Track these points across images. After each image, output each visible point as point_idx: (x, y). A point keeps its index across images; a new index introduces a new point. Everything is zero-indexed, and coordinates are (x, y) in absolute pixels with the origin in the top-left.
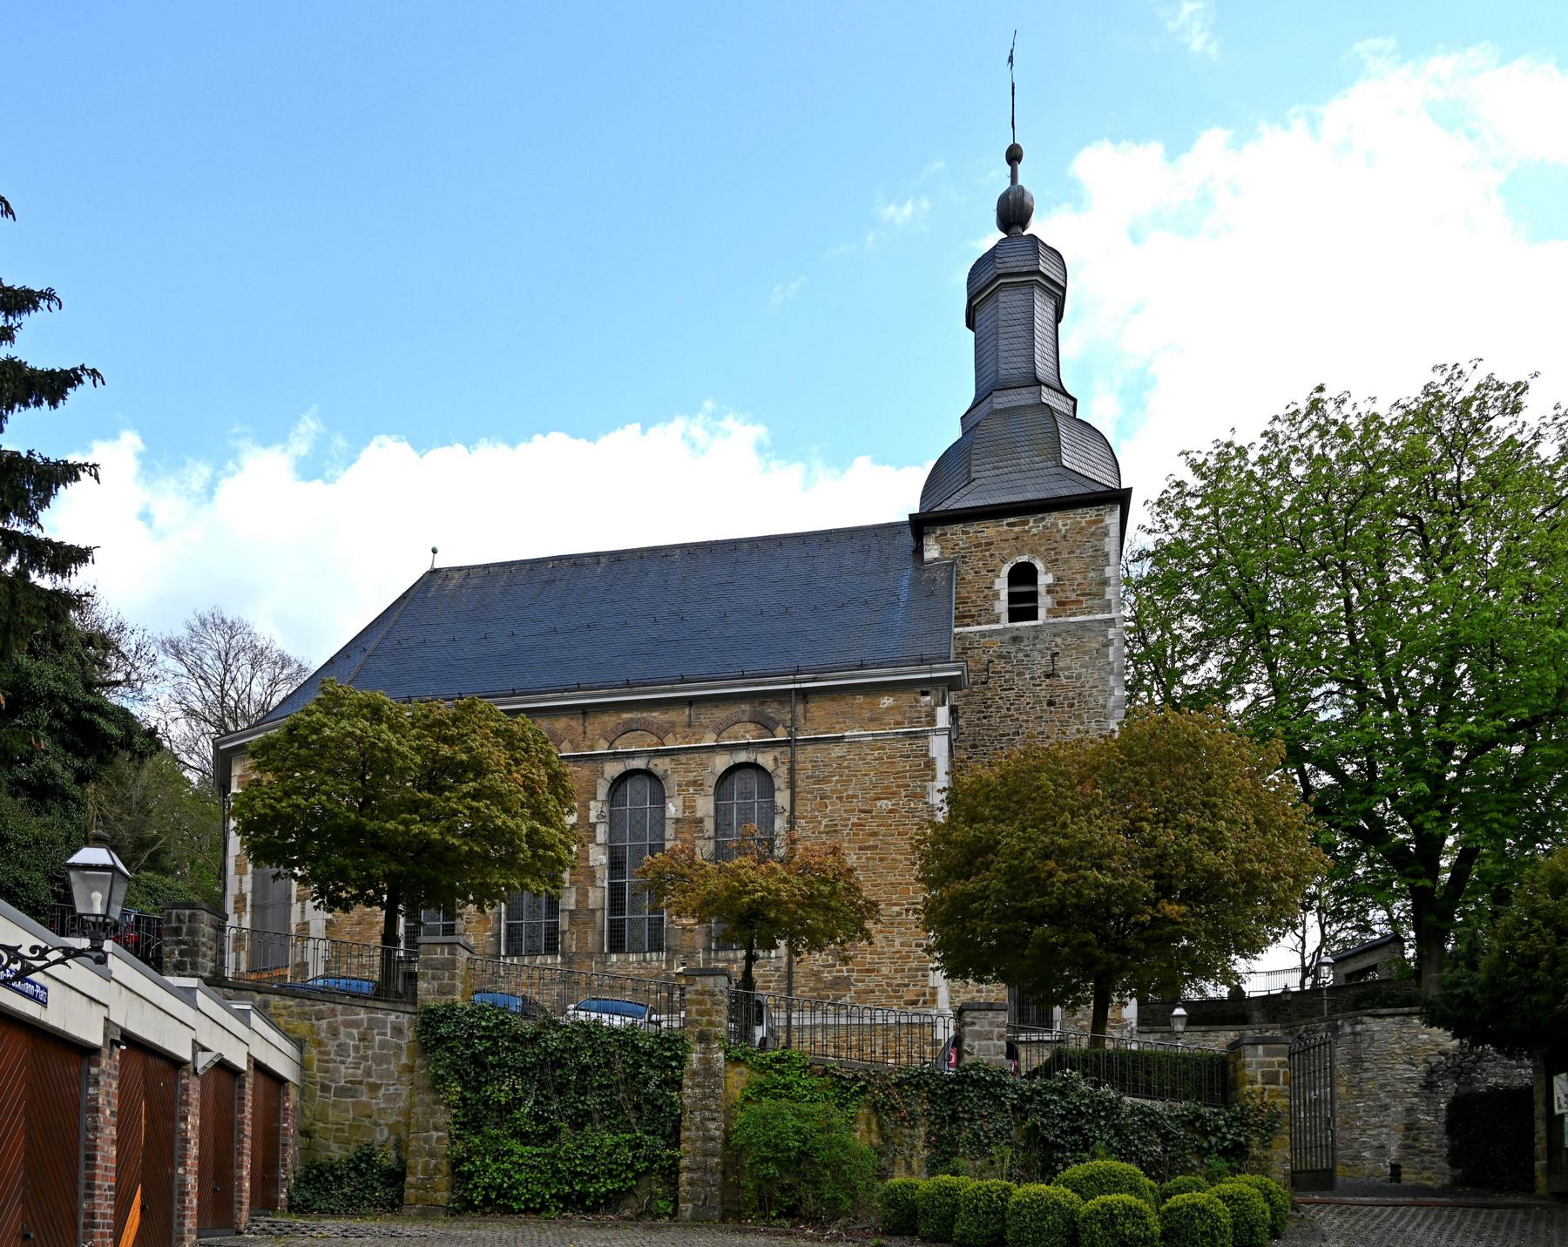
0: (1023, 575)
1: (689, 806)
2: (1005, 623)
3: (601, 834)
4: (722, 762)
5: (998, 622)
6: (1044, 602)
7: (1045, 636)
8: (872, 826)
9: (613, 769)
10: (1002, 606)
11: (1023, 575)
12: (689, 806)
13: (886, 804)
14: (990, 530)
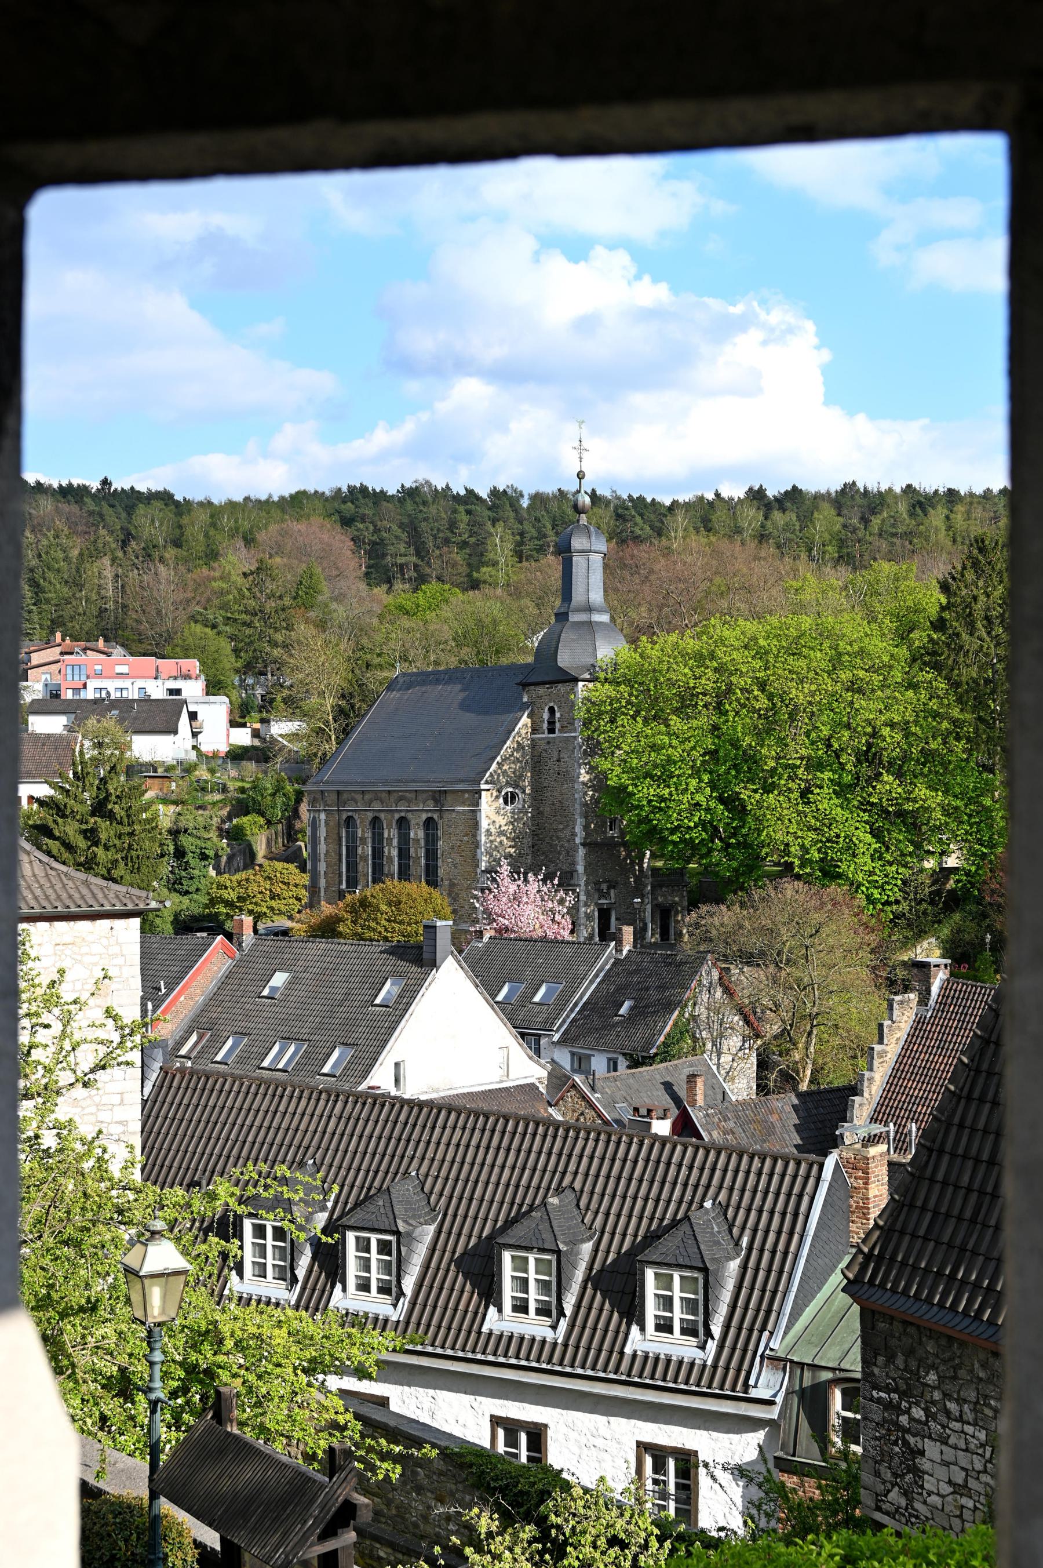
0: (552, 710)
1: (416, 834)
2: (546, 735)
3: (395, 842)
4: (424, 816)
5: (543, 733)
6: (558, 725)
7: (557, 741)
8: (462, 847)
9: (397, 816)
10: (545, 725)
11: (552, 710)
12: (416, 834)
13: (466, 838)
14: (542, 690)
